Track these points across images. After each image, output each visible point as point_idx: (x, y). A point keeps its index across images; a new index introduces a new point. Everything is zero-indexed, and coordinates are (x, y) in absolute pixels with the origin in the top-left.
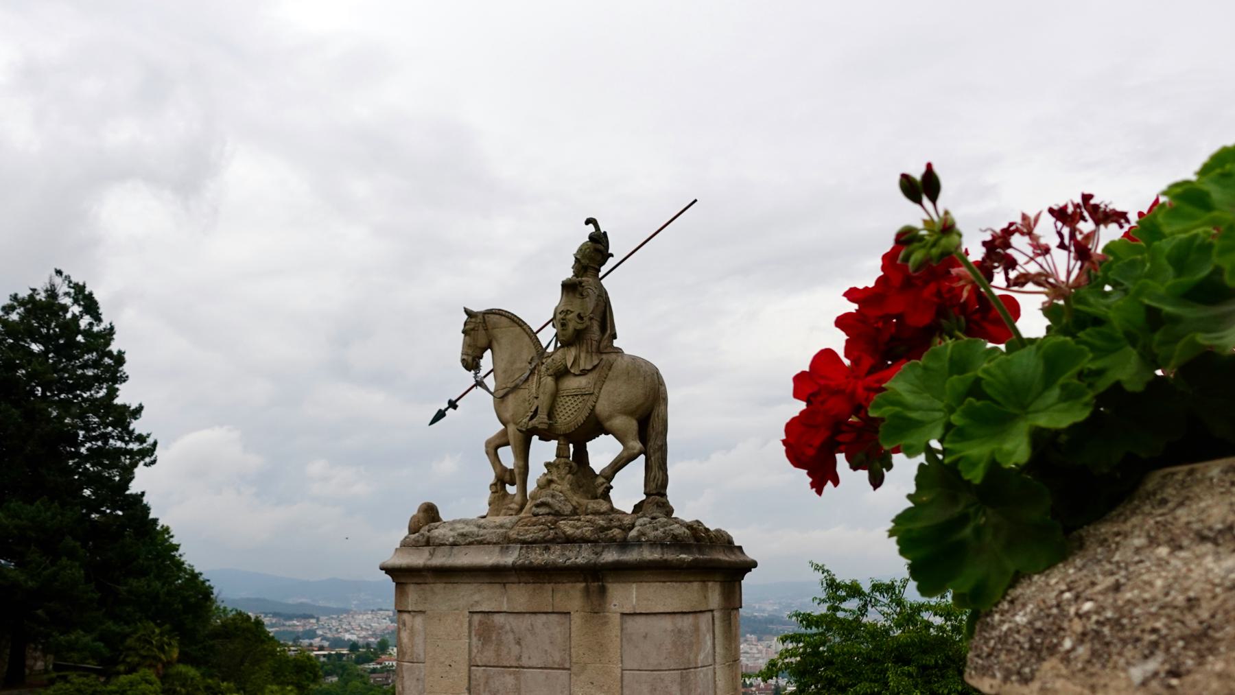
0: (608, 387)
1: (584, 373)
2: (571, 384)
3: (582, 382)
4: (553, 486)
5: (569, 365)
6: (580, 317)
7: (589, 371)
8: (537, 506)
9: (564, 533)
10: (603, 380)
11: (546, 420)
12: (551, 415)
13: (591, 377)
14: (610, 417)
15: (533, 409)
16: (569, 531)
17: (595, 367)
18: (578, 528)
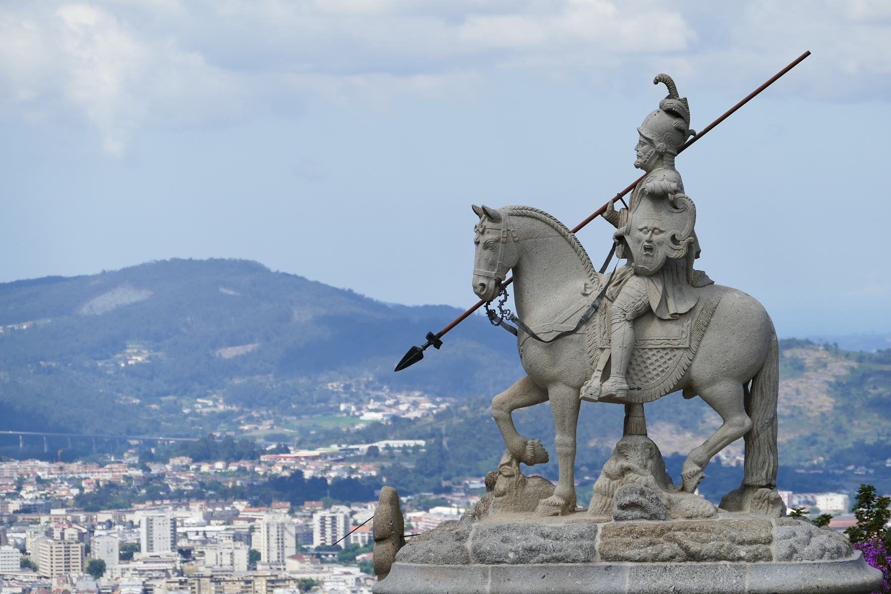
0: (711, 339)
1: (676, 317)
2: (655, 332)
3: (673, 329)
4: (631, 476)
5: (654, 307)
6: (673, 239)
7: (681, 315)
8: (623, 507)
9: (686, 549)
10: (703, 329)
11: (625, 386)
12: (628, 374)
13: (687, 323)
14: (713, 381)
15: (601, 366)
16: (695, 547)
17: (691, 310)
18: (703, 542)
